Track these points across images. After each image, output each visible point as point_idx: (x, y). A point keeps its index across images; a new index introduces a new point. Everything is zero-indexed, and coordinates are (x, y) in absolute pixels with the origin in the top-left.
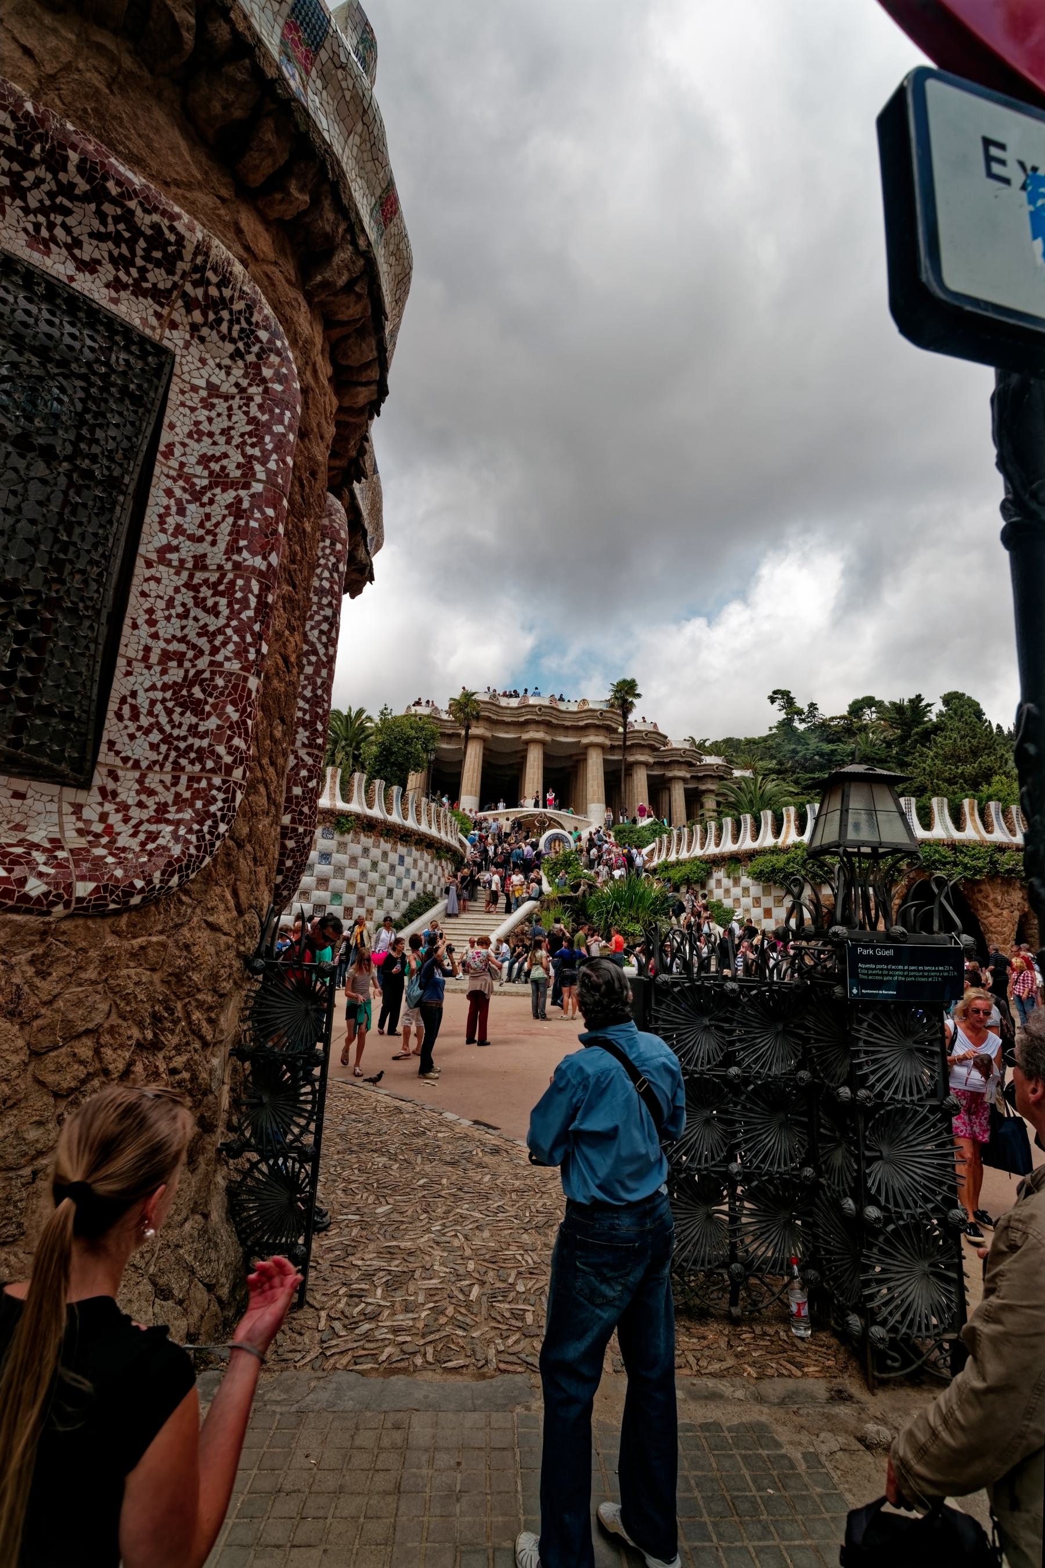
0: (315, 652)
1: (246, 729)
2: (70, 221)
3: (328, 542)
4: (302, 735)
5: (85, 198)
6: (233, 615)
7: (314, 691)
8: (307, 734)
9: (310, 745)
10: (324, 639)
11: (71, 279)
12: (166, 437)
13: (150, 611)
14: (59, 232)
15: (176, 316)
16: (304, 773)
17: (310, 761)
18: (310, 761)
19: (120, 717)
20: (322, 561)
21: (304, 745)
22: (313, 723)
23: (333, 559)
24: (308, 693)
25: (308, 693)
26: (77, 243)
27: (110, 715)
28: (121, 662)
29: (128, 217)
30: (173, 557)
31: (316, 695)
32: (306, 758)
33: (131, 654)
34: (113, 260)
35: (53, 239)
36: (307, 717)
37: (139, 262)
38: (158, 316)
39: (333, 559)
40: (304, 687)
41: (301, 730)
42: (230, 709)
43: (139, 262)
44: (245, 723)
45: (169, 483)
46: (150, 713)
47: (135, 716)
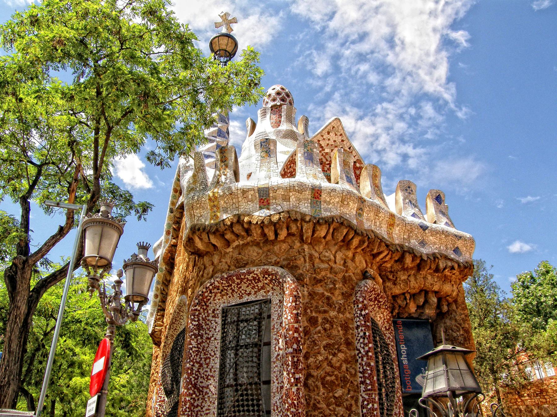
0: (360, 352)
1: (295, 405)
2: (242, 288)
3: (356, 306)
4: (362, 387)
5: (241, 282)
6: (287, 370)
7: (363, 368)
8: (364, 386)
9: (366, 390)
10: (362, 345)
11: (248, 299)
12: (272, 324)
13: (277, 376)
14: (243, 292)
15: (268, 289)
16: (366, 403)
17: (367, 397)
18: (367, 397)
19: (274, 410)
20: (356, 315)
21: (364, 391)
22: (365, 381)
23: (359, 312)
24: (361, 370)
25: (361, 370)
26: (246, 291)
27: (272, 410)
28: (272, 394)
29: (248, 280)
30: (279, 357)
31: (364, 370)
32: (365, 396)
33: (274, 391)
34: (252, 288)
35: (243, 294)
36: (363, 380)
37: (256, 285)
38: (265, 292)
39: (359, 312)
40: (360, 368)
41: (362, 385)
42: (289, 400)
43: (256, 285)
44: (293, 403)
45: (275, 336)
46: (280, 407)
47: (277, 409)
